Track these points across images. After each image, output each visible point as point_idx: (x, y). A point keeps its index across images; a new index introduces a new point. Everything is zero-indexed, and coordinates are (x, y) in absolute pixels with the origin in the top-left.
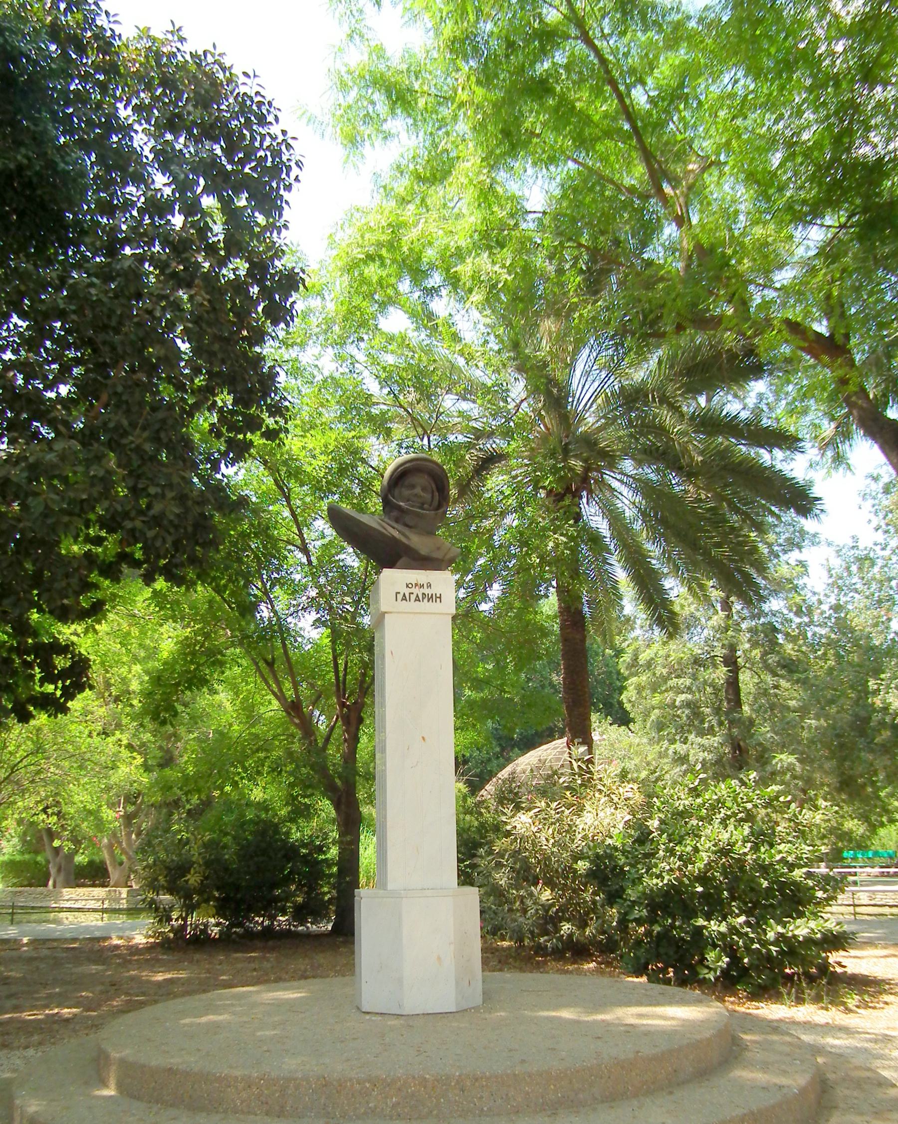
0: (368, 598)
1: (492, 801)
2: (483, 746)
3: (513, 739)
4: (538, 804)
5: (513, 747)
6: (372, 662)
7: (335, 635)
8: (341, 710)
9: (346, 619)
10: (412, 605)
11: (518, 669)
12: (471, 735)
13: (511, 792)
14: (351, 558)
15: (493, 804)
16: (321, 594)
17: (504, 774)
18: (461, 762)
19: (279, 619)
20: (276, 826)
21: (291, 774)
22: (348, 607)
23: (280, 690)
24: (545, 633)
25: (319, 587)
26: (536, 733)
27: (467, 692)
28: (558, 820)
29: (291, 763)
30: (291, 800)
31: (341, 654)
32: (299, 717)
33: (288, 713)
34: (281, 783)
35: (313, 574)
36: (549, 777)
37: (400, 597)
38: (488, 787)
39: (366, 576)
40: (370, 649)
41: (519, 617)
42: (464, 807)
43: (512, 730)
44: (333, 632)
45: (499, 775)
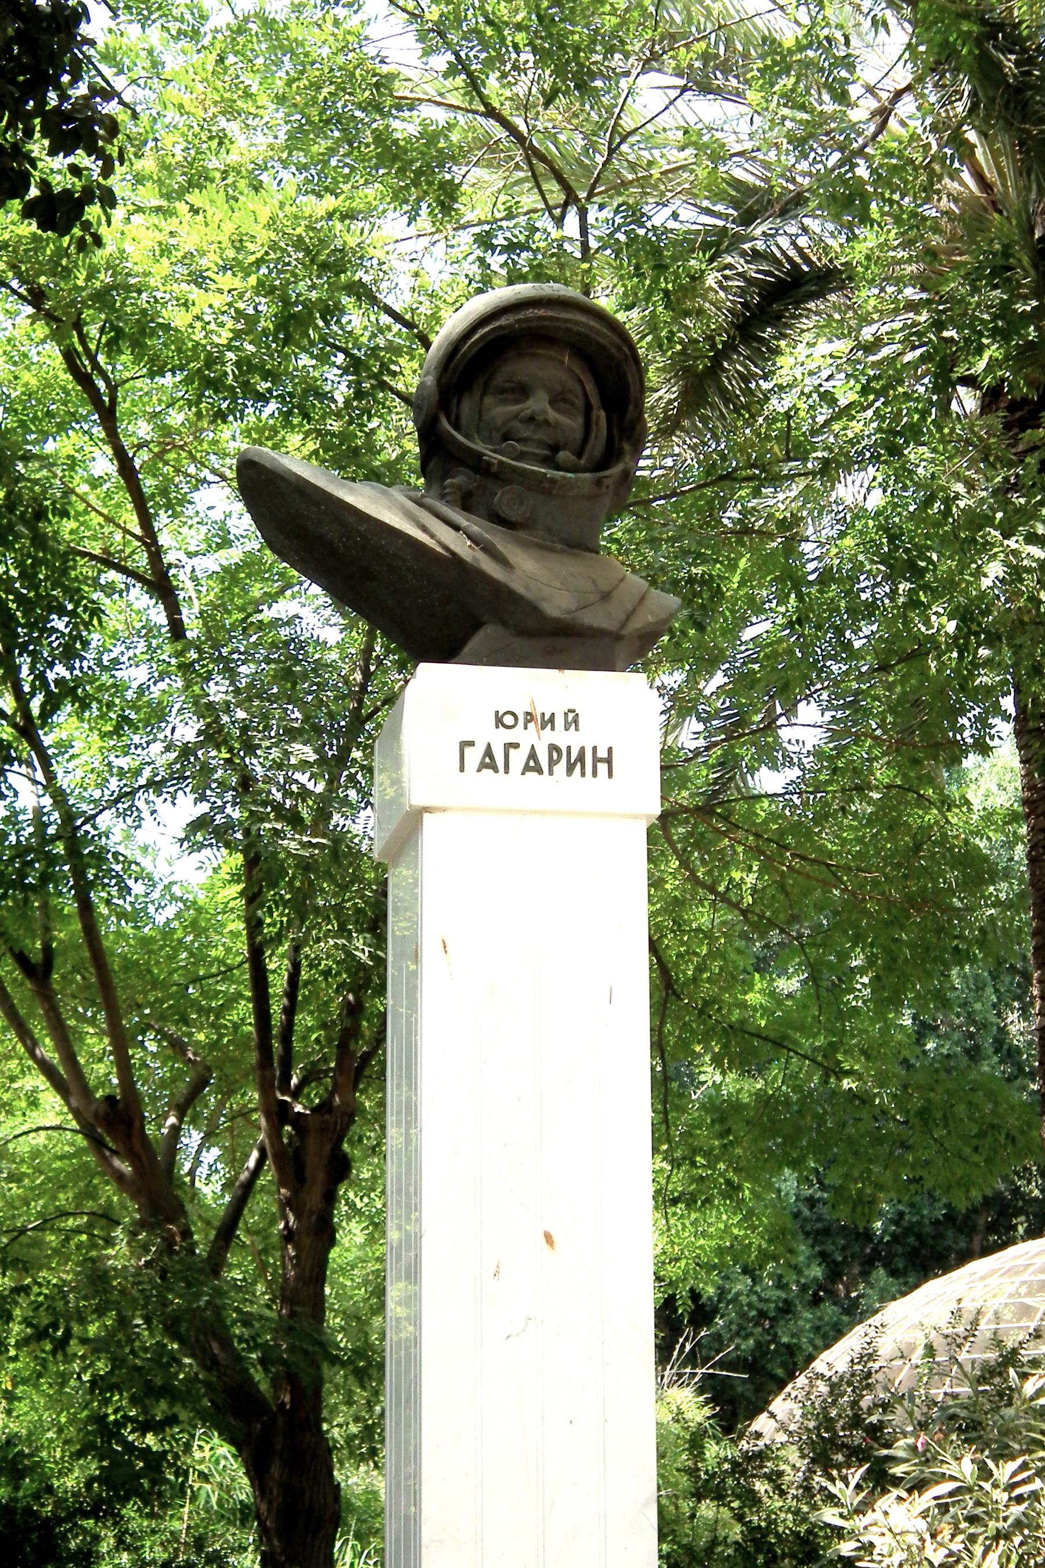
0: (368, 749)
1: (792, 1454)
2: (765, 1256)
3: (867, 1235)
4: (951, 1468)
5: (868, 1264)
6: (381, 963)
7: (259, 872)
8: (275, 1132)
9: (294, 820)
10: (514, 785)
11: (887, 997)
12: (722, 1221)
13: (856, 1421)
14: (312, 614)
15: (793, 1462)
16: (213, 735)
17: (836, 1359)
18: (680, 1321)
19: (69, 818)
20: (47, 1526)
21: (98, 1347)
22: (303, 778)
23: (70, 1058)
24: (977, 870)
25: (206, 709)
26: (950, 1217)
27: (710, 1075)
28: (1018, 1525)
29: (100, 1312)
30: (99, 1437)
31: (278, 939)
32: (131, 1155)
33: (97, 1143)
34: (63, 1379)
35: (186, 668)
36: (990, 1372)
37: (474, 756)
38: (779, 1405)
39: (367, 675)
40: (375, 924)
41: (887, 818)
42: (692, 1472)
43: (867, 1205)
44: (252, 863)
45: (819, 1365)
